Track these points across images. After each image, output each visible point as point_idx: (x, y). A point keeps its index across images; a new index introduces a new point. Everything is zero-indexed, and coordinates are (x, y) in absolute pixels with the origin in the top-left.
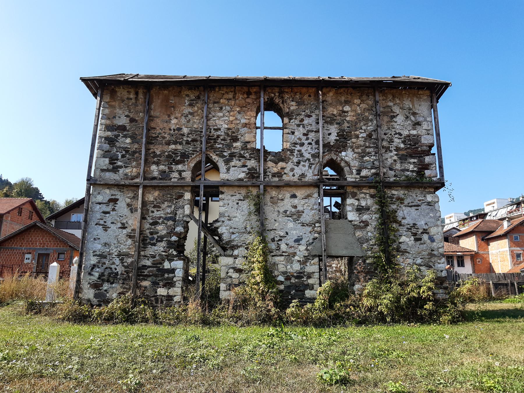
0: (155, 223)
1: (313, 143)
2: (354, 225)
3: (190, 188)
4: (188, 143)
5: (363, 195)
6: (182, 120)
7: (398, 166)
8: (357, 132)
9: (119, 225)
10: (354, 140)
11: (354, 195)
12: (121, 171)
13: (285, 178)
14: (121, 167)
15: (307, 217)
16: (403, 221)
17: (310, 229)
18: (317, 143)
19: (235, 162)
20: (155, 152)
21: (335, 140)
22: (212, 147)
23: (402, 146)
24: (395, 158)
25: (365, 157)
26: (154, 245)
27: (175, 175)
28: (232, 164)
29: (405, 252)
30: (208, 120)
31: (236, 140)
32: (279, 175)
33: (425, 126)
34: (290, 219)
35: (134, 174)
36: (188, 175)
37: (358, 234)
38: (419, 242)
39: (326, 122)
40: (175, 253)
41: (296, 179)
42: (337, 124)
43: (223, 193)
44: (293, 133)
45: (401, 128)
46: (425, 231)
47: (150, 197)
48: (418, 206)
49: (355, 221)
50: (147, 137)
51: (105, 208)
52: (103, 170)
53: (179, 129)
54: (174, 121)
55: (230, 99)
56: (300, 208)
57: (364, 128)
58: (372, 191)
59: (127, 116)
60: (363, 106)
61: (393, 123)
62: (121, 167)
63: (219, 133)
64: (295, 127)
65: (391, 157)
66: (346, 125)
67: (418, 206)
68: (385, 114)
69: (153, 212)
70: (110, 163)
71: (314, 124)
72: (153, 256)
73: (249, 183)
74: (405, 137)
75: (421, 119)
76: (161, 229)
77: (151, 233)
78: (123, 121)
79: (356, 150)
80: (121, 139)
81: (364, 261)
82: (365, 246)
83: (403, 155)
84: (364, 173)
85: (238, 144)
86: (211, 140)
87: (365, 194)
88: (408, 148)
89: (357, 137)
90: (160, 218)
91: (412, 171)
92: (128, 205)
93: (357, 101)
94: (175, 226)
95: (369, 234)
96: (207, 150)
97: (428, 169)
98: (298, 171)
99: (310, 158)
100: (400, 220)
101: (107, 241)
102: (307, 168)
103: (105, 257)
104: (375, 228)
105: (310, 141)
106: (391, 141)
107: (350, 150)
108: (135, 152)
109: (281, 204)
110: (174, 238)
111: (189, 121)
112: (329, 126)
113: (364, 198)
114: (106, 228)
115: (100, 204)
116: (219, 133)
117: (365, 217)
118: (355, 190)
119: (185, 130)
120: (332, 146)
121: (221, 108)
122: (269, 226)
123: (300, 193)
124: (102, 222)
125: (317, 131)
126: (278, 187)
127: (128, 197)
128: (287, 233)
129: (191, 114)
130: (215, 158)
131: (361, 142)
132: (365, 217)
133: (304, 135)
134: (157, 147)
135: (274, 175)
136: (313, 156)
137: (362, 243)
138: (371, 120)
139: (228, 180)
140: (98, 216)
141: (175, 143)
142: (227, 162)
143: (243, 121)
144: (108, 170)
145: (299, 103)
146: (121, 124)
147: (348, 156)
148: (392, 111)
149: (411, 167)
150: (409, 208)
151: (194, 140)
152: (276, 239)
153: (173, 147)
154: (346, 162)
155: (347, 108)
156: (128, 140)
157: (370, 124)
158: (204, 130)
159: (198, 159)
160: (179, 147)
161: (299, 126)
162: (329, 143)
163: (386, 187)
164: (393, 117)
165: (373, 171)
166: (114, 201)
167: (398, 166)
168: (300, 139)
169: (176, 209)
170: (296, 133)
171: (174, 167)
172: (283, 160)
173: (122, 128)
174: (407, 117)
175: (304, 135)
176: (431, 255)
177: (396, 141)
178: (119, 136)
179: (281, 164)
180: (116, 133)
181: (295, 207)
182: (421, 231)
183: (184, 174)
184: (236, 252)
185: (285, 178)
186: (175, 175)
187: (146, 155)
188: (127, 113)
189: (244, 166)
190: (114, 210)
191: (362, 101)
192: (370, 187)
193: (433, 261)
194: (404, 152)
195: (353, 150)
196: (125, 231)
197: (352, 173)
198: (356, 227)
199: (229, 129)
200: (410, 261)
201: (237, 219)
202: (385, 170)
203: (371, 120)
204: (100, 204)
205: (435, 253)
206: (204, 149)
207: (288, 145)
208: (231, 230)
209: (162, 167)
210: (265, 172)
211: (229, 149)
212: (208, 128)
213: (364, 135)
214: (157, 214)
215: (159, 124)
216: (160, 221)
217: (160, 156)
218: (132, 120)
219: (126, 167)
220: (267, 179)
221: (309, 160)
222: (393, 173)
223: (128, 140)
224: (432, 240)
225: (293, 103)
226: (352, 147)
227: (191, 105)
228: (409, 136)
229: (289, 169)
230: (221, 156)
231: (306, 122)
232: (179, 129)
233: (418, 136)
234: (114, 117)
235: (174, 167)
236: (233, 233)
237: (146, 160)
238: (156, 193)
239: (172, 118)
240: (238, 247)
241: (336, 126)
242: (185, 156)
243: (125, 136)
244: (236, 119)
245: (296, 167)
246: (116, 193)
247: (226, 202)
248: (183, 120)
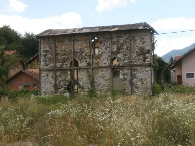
0: (60, 82)
1: (108, 52)
2: (122, 79)
3: (69, 70)
4: (68, 55)
5: (125, 69)
6: (64, 47)
7: (137, 58)
8: (123, 47)
9: (50, 83)
11: (122, 69)
12: (49, 65)
13: (100, 65)
14: (48, 64)
15: (107, 78)
16: (138, 77)
17: (108, 81)
18: (109, 52)
19: (83, 60)
20: (58, 59)
21: (116, 50)
22: (76, 56)
23: (138, 51)
24: (136, 55)
25: (125, 56)
26: (60, 89)
27: (65, 66)
28: (82, 61)
29: (138, 88)
30: (74, 46)
31: (83, 52)
32: (97, 64)
33: (147, 43)
34: (101, 78)
35: (53, 66)
36: (69, 65)
37: (123, 82)
38: (143, 84)
39: (113, 44)
40: (66, 91)
41: (103, 65)
42: (117, 44)
43: (79, 71)
44: (102, 49)
45: (138, 44)
46: (145, 80)
47: (58, 74)
48: (143, 72)
49: (122, 78)
50: (56, 53)
51: (45, 78)
52: (43, 66)
53: (65, 50)
54: (63, 47)
55: (81, 38)
56: (104, 75)
57: (125, 45)
58: (128, 68)
59: (49, 47)
61: (135, 43)
62: (48, 64)
63: (78, 50)
64: (103, 47)
65: (134, 55)
66: (119, 45)
67: (143, 72)
68: (133, 39)
69: (59, 78)
70: (45, 63)
71: (109, 45)
72: (60, 92)
73: (88, 68)
74: (140, 48)
75: (145, 40)
76: (62, 84)
77: (59, 85)
78: (48, 49)
79: (123, 54)
80: (47, 55)
81: (125, 91)
82: (125, 86)
83: (138, 54)
84: (125, 61)
85: (84, 54)
86: (75, 53)
87: (126, 69)
88: (141, 52)
89: (123, 49)
90: (61, 80)
91: (142, 60)
92: (52, 76)
93: (123, 36)
94: (66, 82)
95: (127, 82)
96: (74, 57)
97: (147, 59)
98: (104, 62)
99: (107, 57)
100: (136, 77)
101: (47, 88)
102: (106, 61)
103: (47, 93)
104: (129, 80)
105: (107, 51)
106: (135, 50)
107: (121, 54)
108: (52, 59)
109: (98, 73)
110: (66, 86)
111: (68, 47)
112: (114, 45)
113: (125, 70)
114: (46, 84)
115: (43, 76)
116: (78, 50)
117: (126, 77)
118: (122, 68)
119: (67, 50)
120: (115, 53)
121: (78, 42)
122: (95, 81)
123: (104, 70)
124: (44, 82)
125: (109, 48)
126: (97, 68)
127: (52, 74)
128: (100, 83)
129: (68, 44)
130: (77, 59)
131: (124, 50)
132: (126, 77)
133: (106, 49)
134: (59, 56)
135: (96, 64)
136: (109, 56)
137: (124, 86)
138: (128, 42)
139: (81, 67)
140: (44, 80)
141: (64, 55)
142: (81, 60)
143: (85, 46)
144: (45, 66)
145: (104, 38)
146: (47, 50)
147: (120, 55)
148: (135, 39)
149: (141, 58)
150: (140, 73)
151: (70, 54)
152: (97, 85)
153: (63, 56)
154: (119, 58)
155: (120, 39)
156: (50, 55)
157: (128, 44)
158: (73, 50)
159: (71, 60)
160: (65, 56)
161: (104, 46)
162: (114, 51)
163: (132, 66)
164: (135, 41)
165: (128, 61)
166: (47, 75)
167: (137, 58)
168: (104, 51)
169: (66, 77)
170: (103, 49)
171: (64, 63)
172: (98, 59)
173: (48, 51)
175: (106, 49)
176: (147, 89)
177: (136, 49)
178: (47, 54)
179: (98, 60)
180: (46, 53)
181: (103, 74)
182: (143, 80)
183: (68, 65)
184: (85, 90)
185: (100, 65)
186: (65, 66)
187: (56, 60)
188: (49, 46)
189: (86, 61)
190: (47, 78)
191: (125, 35)
192: (127, 66)
193: (147, 90)
194: (139, 53)
195: (122, 54)
196: (52, 85)
197: (121, 62)
198: (123, 80)
199: (81, 49)
200: (139, 90)
201: (85, 80)
202: (132, 60)
203: (128, 42)
204: (43, 76)
205: (148, 87)
206: (73, 57)
207: (100, 53)
208: (83, 83)
209: (61, 63)
210: (93, 63)
211: (81, 56)
212: (74, 49)
213: (126, 48)
214: (60, 79)
215: (59, 49)
216: (61, 81)
217: (60, 60)
218: (50, 48)
219: (50, 64)
220: (94, 66)
221: (107, 58)
222: (135, 61)
223: (50, 55)
224: (147, 83)
225: (102, 38)
226: (121, 53)
227: (68, 41)
228: (141, 47)
229: (100, 61)
230: (79, 58)
231: (106, 44)
232: (65, 50)
233: (144, 47)
234: (45, 48)
235: (64, 63)
236: (83, 84)
237: (56, 61)
238: (59, 72)
239: (63, 46)
240: (85, 88)
241: (116, 45)
242: (67, 59)
243: (49, 54)
244: (83, 45)
245: (103, 61)
246: (47, 73)
247: (81, 74)
248: (66, 47)
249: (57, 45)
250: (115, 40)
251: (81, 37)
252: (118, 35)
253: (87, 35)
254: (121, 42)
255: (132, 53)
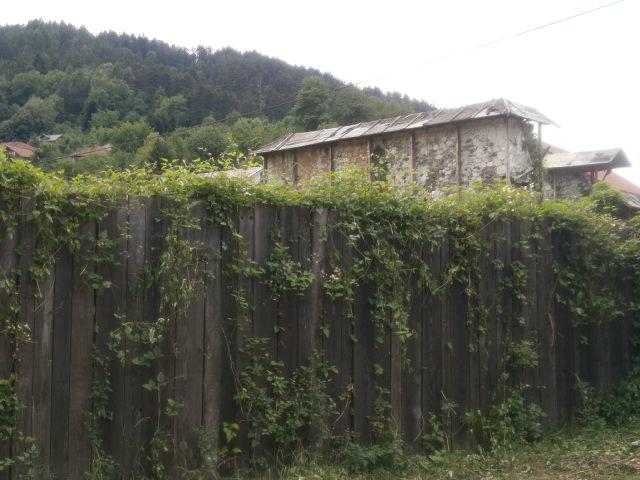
10: (441, 179)
23: (480, 179)
33: (501, 156)
60: (449, 143)
68: (467, 148)
75: (497, 149)
89: (443, 175)
93: (444, 139)
131: (445, 179)
145: (399, 148)
148: (472, 146)
155: (435, 147)
161: (399, 170)
164: (472, 151)
174: (486, 149)
177: (475, 174)
213: (450, 172)
228: (485, 169)
233: (493, 168)
249: (300, 173)
250: (424, 151)
251: (349, 148)
252: (432, 138)
253: (362, 144)
254: (439, 157)
255: (464, 186)
